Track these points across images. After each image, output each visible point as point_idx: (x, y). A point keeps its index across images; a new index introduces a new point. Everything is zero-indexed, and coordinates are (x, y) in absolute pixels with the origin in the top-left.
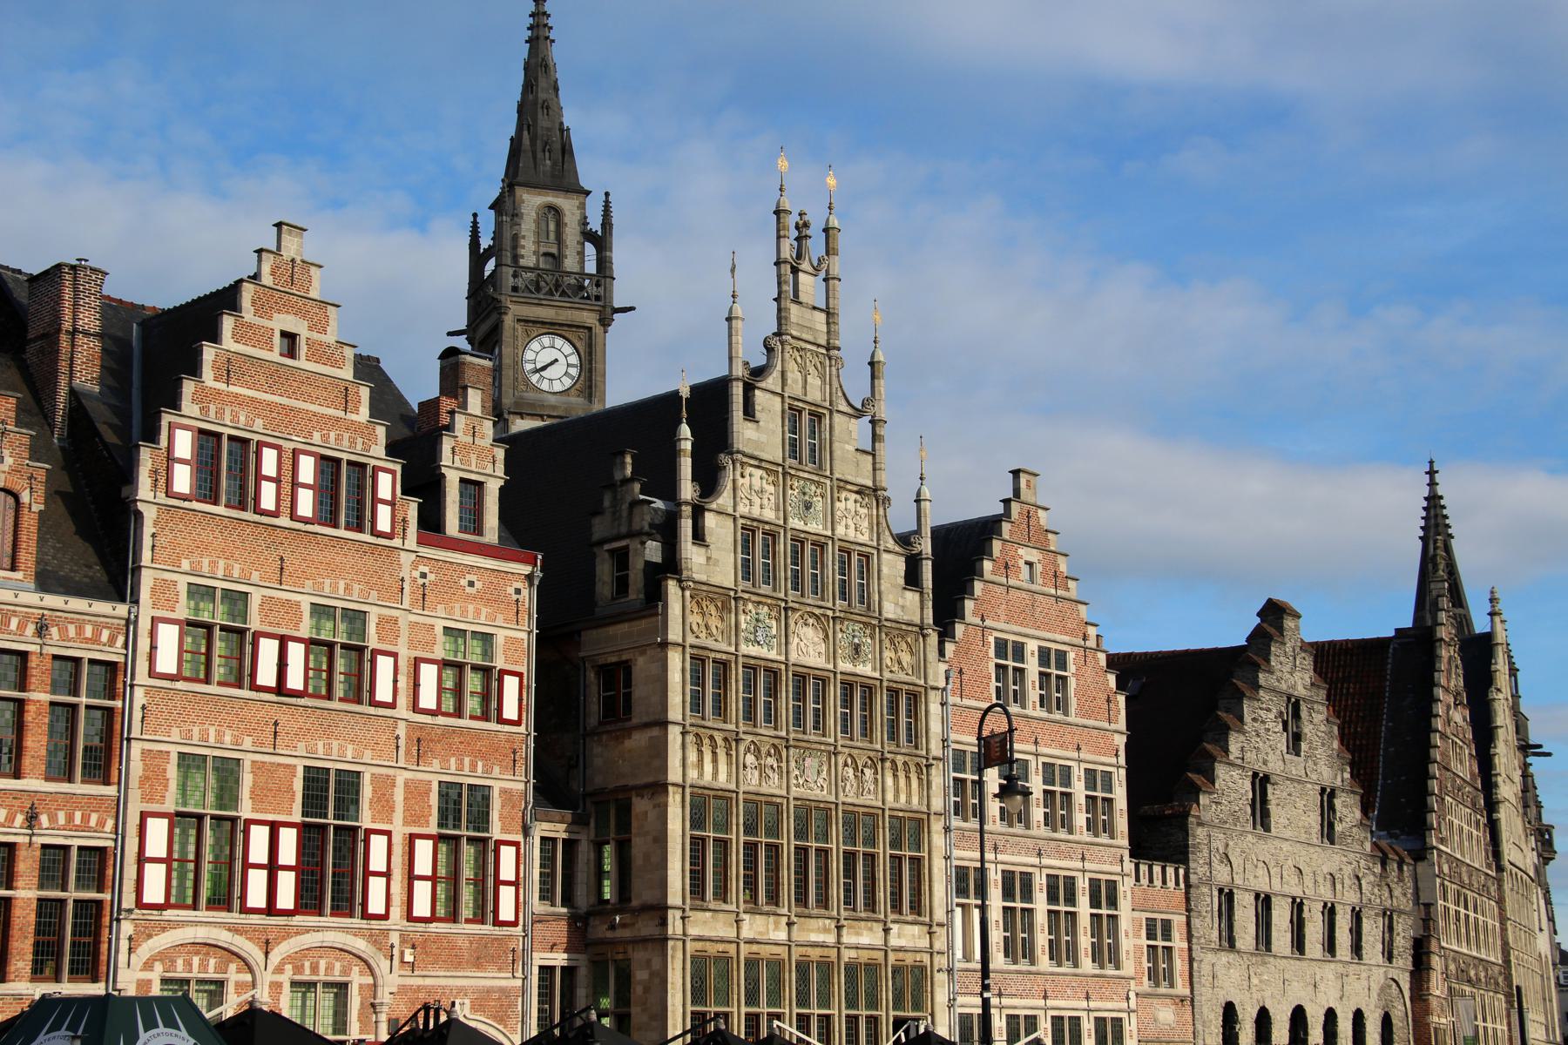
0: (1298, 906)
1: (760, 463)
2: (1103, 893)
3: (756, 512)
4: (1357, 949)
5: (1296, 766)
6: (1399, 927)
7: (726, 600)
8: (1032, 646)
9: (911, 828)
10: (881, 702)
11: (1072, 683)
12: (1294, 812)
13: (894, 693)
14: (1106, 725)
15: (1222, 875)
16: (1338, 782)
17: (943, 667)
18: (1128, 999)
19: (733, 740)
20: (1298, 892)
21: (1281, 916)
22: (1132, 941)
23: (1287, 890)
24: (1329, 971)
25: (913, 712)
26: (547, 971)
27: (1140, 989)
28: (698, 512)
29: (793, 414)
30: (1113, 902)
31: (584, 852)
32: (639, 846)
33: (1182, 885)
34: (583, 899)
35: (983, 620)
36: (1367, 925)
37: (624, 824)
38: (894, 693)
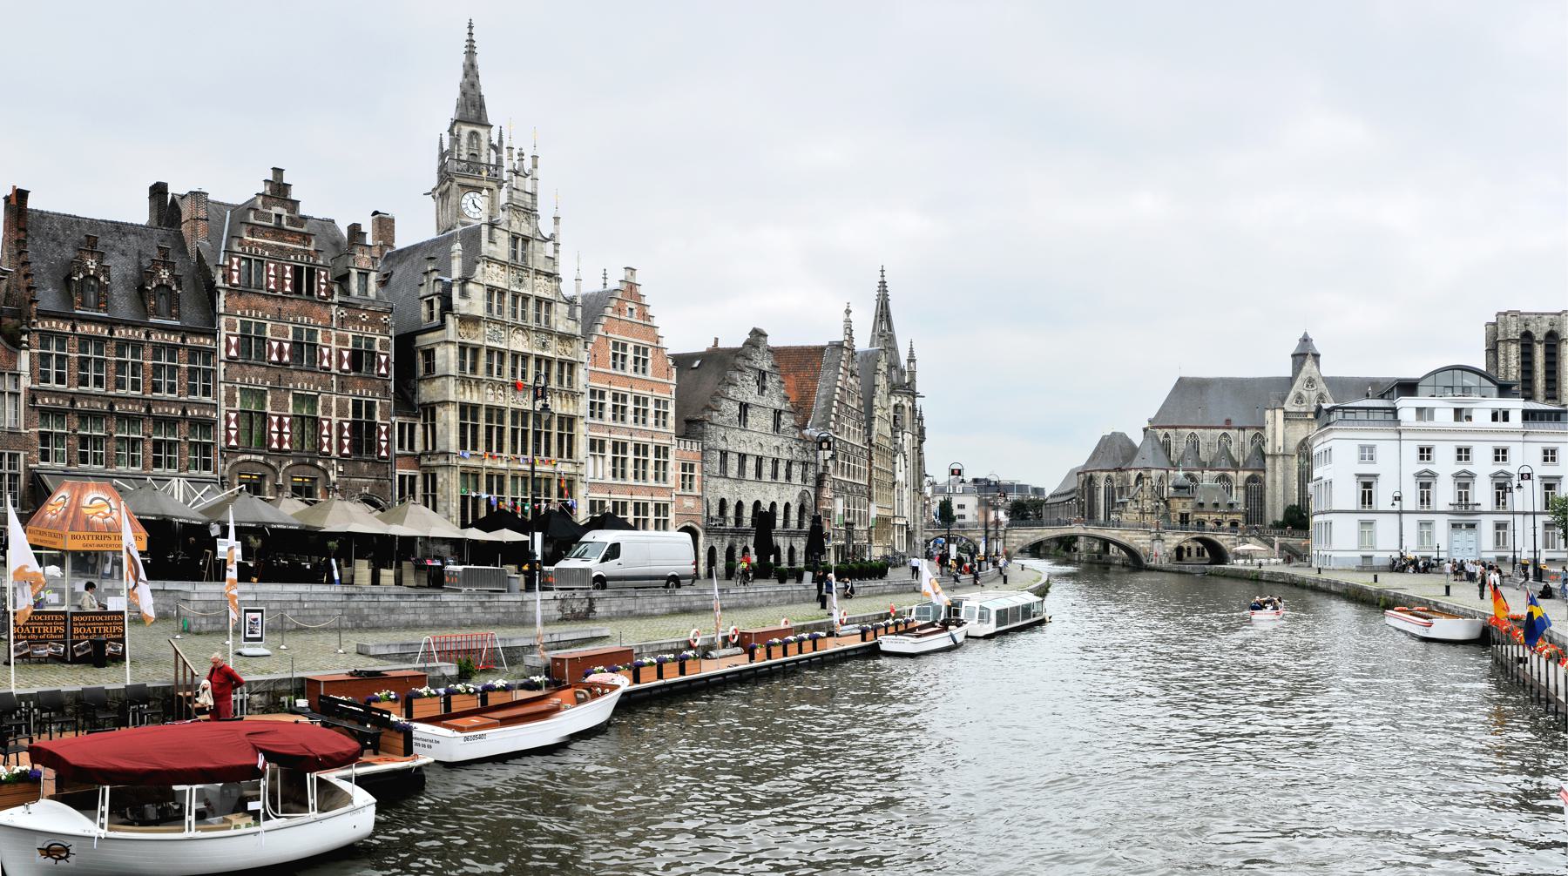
0: (759, 460)
1: (497, 262)
2: (662, 451)
3: (494, 283)
4: (788, 477)
5: (763, 401)
6: (811, 468)
8: (630, 346)
9: (568, 422)
11: (650, 362)
12: (760, 421)
15: (723, 446)
19: (479, 382)
21: (751, 464)
22: (674, 471)
24: (774, 487)
25: (571, 372)
26: (402, 478)
28: (465, 281)
29: (514, 238)
30: (666, 456)
31: (419, 429)
32: (439, 426)
34: (419, 448)
36: (794, 468)
37: (433, 419)
38: (561, 363)
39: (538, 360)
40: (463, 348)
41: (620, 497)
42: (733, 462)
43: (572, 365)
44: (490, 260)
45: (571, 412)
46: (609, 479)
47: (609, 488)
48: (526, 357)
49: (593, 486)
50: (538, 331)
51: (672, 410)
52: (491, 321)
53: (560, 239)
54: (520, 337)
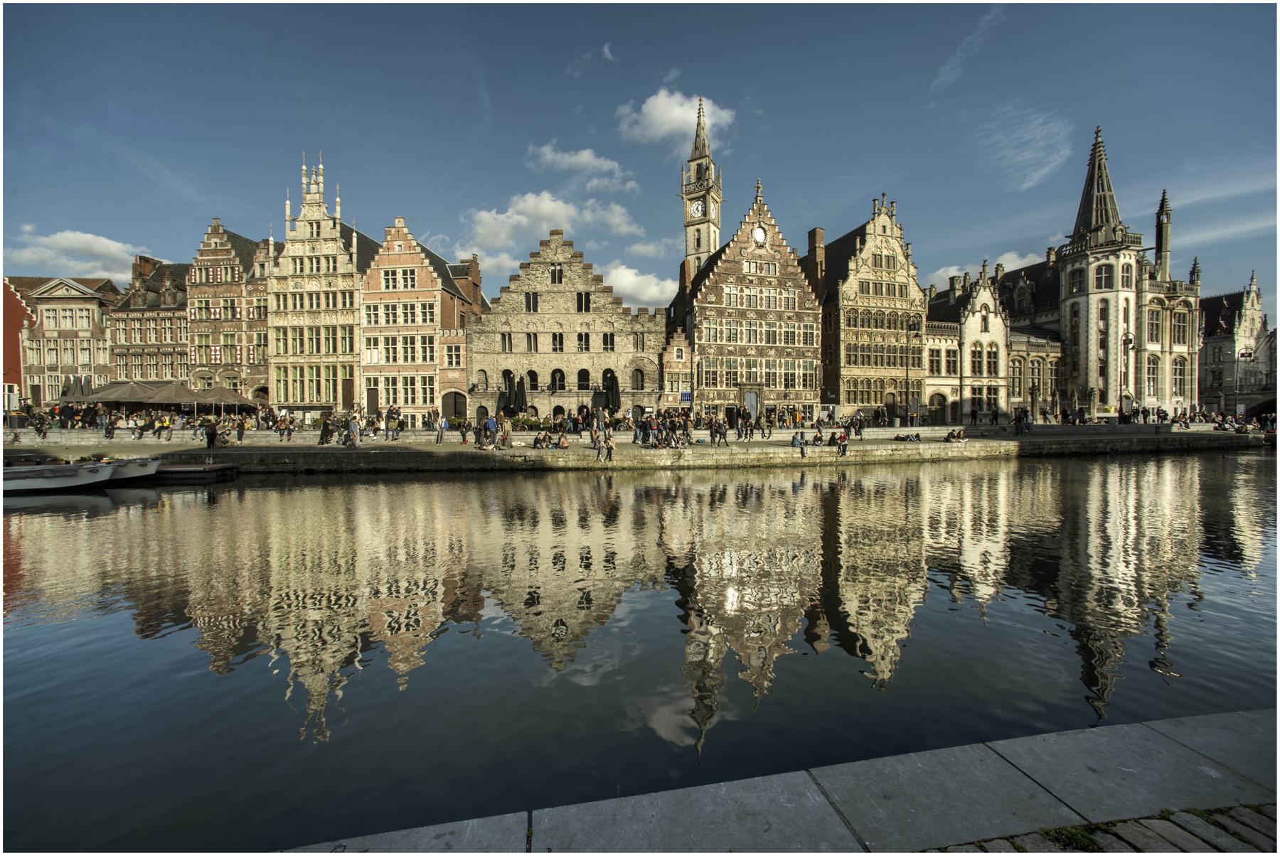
7: (285, 278)
10: (339, 296)
13: (344, 294)
15: (506, 329)
16: (593, 289)
19: (286, 314)
20: (557, 330)
22: (440, 352)
29: (311, 225)
36: (616, 339)
39: (327, 294)
40: (278, 296)
41: (390, 375)
42: (520, 343)
44: (294, 241)
45: (351, 322)
46: (383, 362)
47: (380, 369)
49: (366, 368)
50: (326, 276)
51: (437, 310)
52: (294, 276)
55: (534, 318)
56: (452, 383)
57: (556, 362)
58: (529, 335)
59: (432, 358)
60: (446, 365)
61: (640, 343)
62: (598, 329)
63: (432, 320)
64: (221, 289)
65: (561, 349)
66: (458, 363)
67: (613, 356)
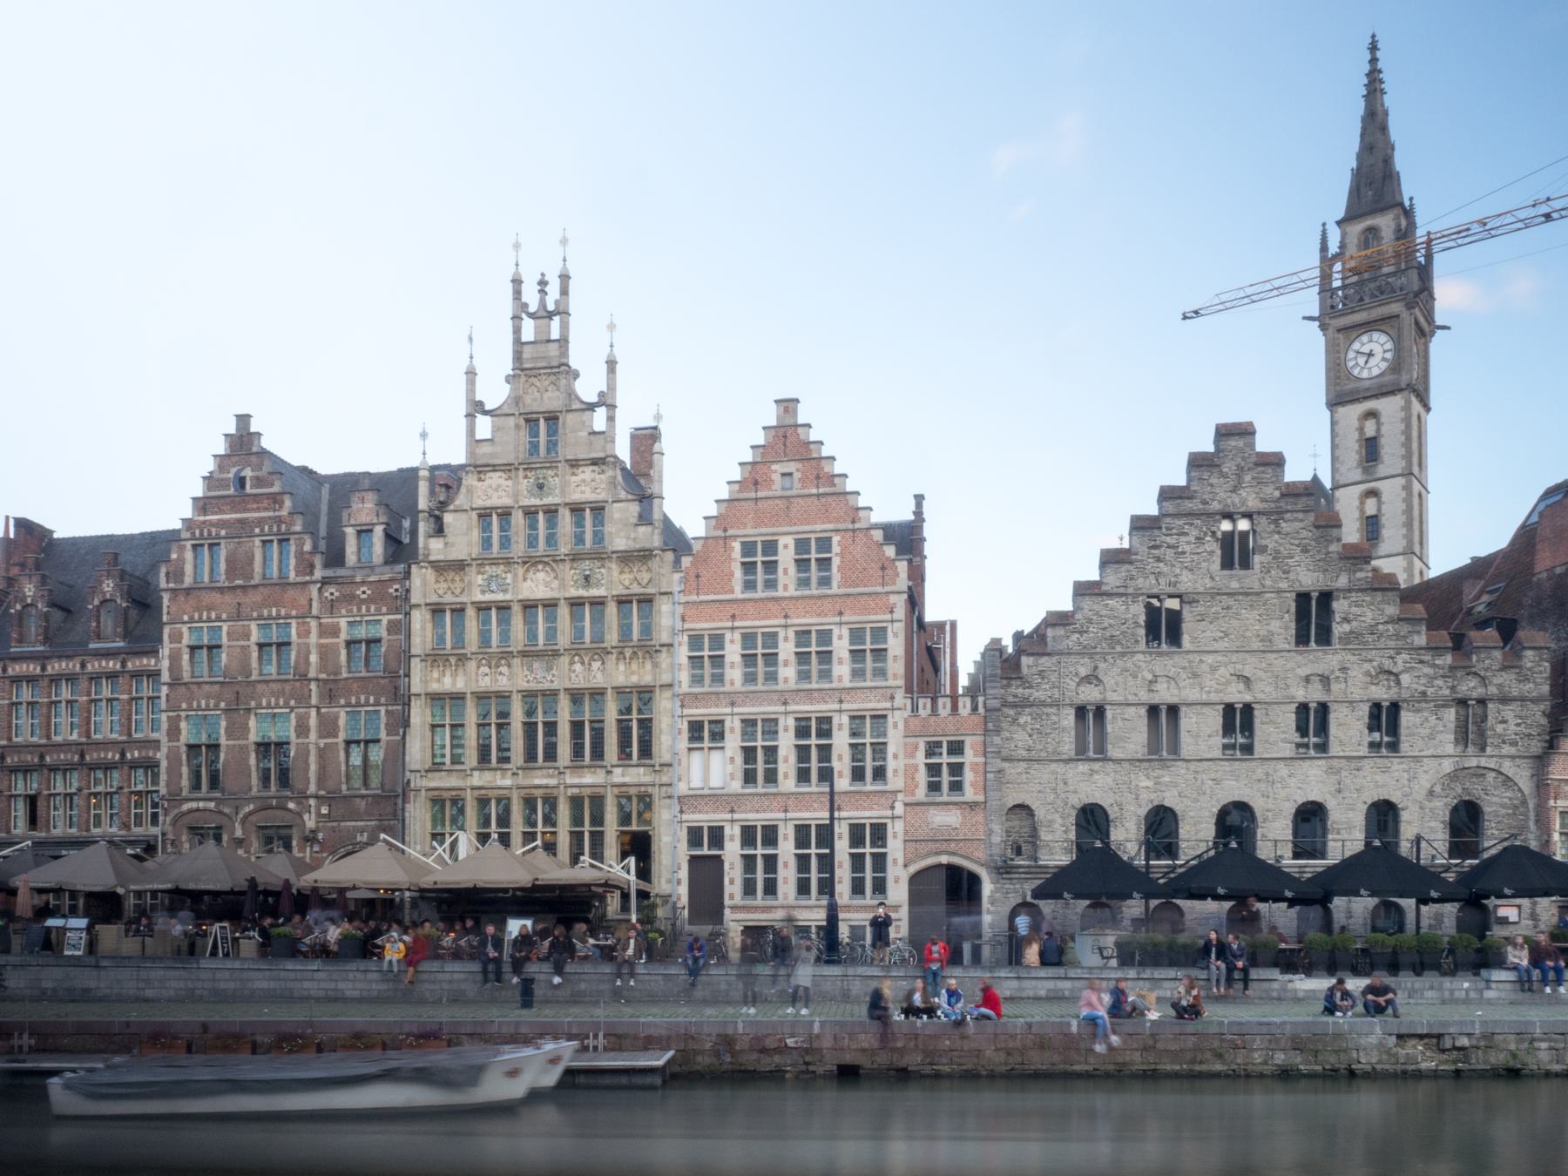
3: (488, 503)
5: (1235, 580)
7: (460, 566)
11: (836, 562)
14: (879, 589)
15: (1090, 695)
17: (677, 576)
18: (892, 808)
19: (462, 659)
20: (1237, 695)
22: (905, 761)
23: (1214, 697)
27: (909, 799)
33: (981, 710)
35: (725, 530)
36: (1407, 718)
38: (623, 602)
39: (576, 604)
40: (437, 610)
41: (758, 818)
42: (1128, 732)
43: (646, 601)
45: (647, 679)
46: (736, 786)
48: (551, 605)
49: (687, 802)
50: (575, 558)
52: (482, 562)
53: (621, 399)
54: (541, 575)
55: (1168, 663)
56: (941, 840)
57: (1235, 784)
58: (1153, 710)
59: (879, 773)
60: (921, 793)
61: (1472, 731)
62: (1357, 693)
63: (880, 673)
64: (255, 597)
65: (1248, 749)
66: (956, 787)
67: (1397, 766)
